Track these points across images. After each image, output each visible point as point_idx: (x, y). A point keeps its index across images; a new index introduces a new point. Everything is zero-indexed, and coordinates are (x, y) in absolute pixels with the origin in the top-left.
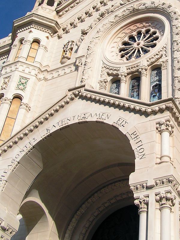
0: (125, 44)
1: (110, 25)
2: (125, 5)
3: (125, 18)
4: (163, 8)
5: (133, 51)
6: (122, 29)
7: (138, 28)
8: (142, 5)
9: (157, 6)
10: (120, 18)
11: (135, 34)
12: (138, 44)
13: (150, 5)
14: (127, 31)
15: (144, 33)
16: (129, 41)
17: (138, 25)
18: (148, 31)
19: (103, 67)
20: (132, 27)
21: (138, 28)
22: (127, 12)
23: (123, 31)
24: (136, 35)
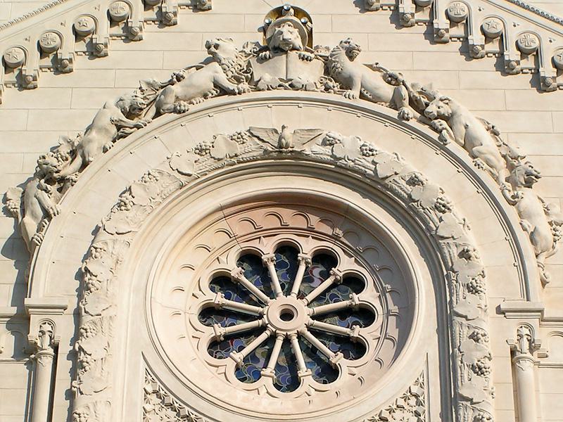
0: (222, 281)
1: (176, 185)
2: (238, 98)
3: (239, 168)
4: (410, 196)
5: (264, 336)
6: (220, 214)
7: (285, 227)
8: (320, 140)
9: (387, 177)
10: (219, 164)
11: (267, 249)
12: (287, 315)
13: (356, 155)
14: (238, 226)
15: (307, 263)
16: (243, 278)
17: (287, 214)
18: (325, 259)
19: (150, 389)
20: (261, 217)
21: (285, 227)
22: (251, 148)
23: (223, 225)
24: (272, 261)
